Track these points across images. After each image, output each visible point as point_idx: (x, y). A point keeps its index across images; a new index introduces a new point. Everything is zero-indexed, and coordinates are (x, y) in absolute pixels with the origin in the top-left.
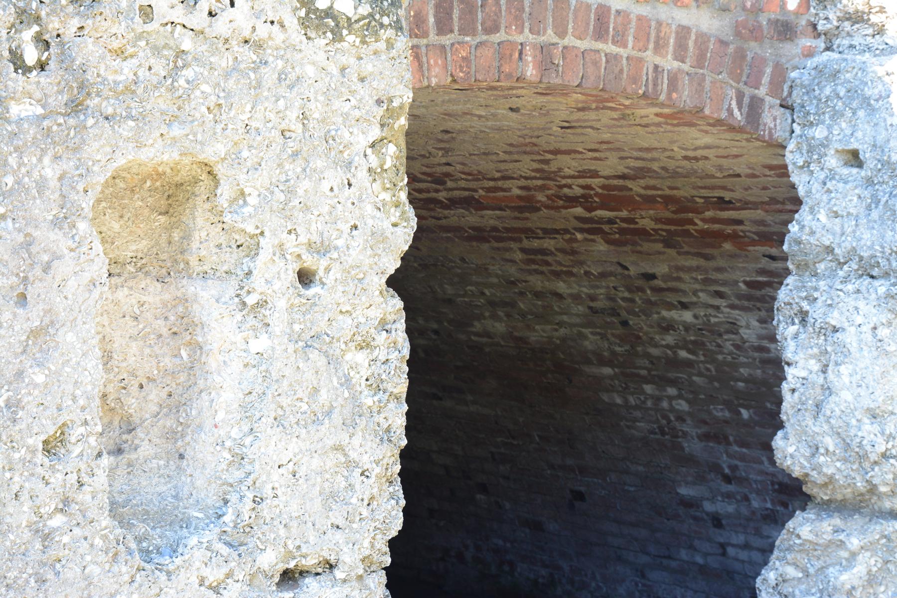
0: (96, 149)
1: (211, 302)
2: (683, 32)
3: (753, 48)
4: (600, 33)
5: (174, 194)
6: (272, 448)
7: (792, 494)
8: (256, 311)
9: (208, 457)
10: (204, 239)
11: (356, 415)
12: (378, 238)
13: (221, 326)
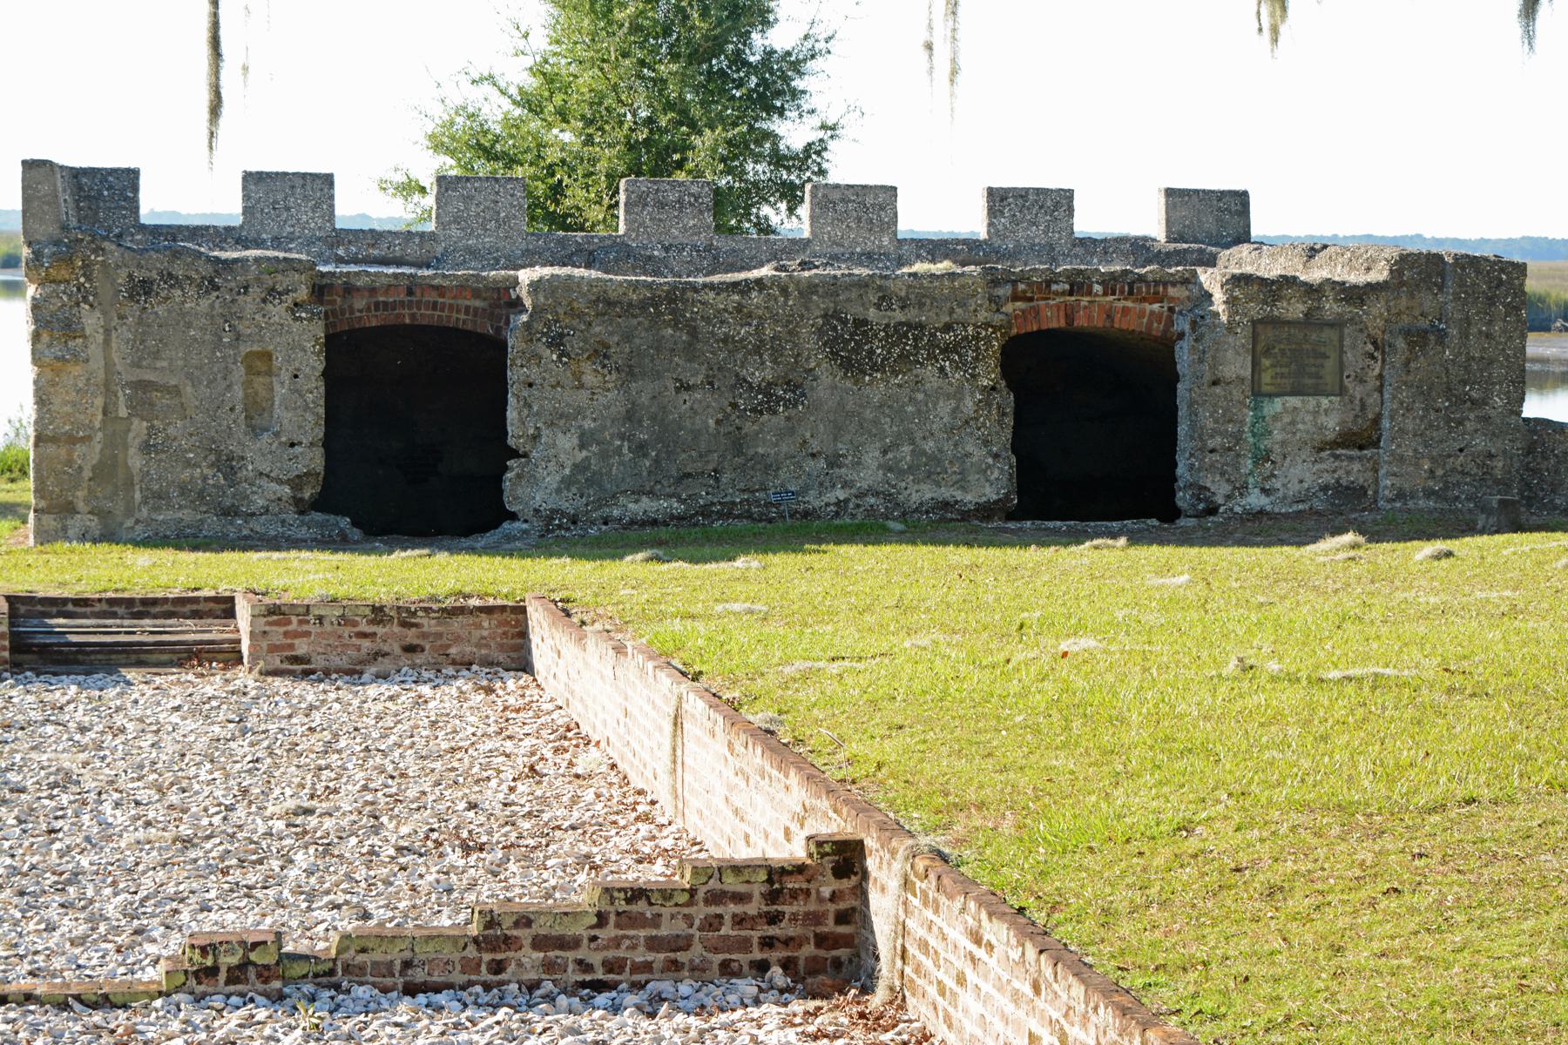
0: (242, 348)
2: (467, 308)
3: (497, 311)
11: (306, 408)
13: (277, 387)
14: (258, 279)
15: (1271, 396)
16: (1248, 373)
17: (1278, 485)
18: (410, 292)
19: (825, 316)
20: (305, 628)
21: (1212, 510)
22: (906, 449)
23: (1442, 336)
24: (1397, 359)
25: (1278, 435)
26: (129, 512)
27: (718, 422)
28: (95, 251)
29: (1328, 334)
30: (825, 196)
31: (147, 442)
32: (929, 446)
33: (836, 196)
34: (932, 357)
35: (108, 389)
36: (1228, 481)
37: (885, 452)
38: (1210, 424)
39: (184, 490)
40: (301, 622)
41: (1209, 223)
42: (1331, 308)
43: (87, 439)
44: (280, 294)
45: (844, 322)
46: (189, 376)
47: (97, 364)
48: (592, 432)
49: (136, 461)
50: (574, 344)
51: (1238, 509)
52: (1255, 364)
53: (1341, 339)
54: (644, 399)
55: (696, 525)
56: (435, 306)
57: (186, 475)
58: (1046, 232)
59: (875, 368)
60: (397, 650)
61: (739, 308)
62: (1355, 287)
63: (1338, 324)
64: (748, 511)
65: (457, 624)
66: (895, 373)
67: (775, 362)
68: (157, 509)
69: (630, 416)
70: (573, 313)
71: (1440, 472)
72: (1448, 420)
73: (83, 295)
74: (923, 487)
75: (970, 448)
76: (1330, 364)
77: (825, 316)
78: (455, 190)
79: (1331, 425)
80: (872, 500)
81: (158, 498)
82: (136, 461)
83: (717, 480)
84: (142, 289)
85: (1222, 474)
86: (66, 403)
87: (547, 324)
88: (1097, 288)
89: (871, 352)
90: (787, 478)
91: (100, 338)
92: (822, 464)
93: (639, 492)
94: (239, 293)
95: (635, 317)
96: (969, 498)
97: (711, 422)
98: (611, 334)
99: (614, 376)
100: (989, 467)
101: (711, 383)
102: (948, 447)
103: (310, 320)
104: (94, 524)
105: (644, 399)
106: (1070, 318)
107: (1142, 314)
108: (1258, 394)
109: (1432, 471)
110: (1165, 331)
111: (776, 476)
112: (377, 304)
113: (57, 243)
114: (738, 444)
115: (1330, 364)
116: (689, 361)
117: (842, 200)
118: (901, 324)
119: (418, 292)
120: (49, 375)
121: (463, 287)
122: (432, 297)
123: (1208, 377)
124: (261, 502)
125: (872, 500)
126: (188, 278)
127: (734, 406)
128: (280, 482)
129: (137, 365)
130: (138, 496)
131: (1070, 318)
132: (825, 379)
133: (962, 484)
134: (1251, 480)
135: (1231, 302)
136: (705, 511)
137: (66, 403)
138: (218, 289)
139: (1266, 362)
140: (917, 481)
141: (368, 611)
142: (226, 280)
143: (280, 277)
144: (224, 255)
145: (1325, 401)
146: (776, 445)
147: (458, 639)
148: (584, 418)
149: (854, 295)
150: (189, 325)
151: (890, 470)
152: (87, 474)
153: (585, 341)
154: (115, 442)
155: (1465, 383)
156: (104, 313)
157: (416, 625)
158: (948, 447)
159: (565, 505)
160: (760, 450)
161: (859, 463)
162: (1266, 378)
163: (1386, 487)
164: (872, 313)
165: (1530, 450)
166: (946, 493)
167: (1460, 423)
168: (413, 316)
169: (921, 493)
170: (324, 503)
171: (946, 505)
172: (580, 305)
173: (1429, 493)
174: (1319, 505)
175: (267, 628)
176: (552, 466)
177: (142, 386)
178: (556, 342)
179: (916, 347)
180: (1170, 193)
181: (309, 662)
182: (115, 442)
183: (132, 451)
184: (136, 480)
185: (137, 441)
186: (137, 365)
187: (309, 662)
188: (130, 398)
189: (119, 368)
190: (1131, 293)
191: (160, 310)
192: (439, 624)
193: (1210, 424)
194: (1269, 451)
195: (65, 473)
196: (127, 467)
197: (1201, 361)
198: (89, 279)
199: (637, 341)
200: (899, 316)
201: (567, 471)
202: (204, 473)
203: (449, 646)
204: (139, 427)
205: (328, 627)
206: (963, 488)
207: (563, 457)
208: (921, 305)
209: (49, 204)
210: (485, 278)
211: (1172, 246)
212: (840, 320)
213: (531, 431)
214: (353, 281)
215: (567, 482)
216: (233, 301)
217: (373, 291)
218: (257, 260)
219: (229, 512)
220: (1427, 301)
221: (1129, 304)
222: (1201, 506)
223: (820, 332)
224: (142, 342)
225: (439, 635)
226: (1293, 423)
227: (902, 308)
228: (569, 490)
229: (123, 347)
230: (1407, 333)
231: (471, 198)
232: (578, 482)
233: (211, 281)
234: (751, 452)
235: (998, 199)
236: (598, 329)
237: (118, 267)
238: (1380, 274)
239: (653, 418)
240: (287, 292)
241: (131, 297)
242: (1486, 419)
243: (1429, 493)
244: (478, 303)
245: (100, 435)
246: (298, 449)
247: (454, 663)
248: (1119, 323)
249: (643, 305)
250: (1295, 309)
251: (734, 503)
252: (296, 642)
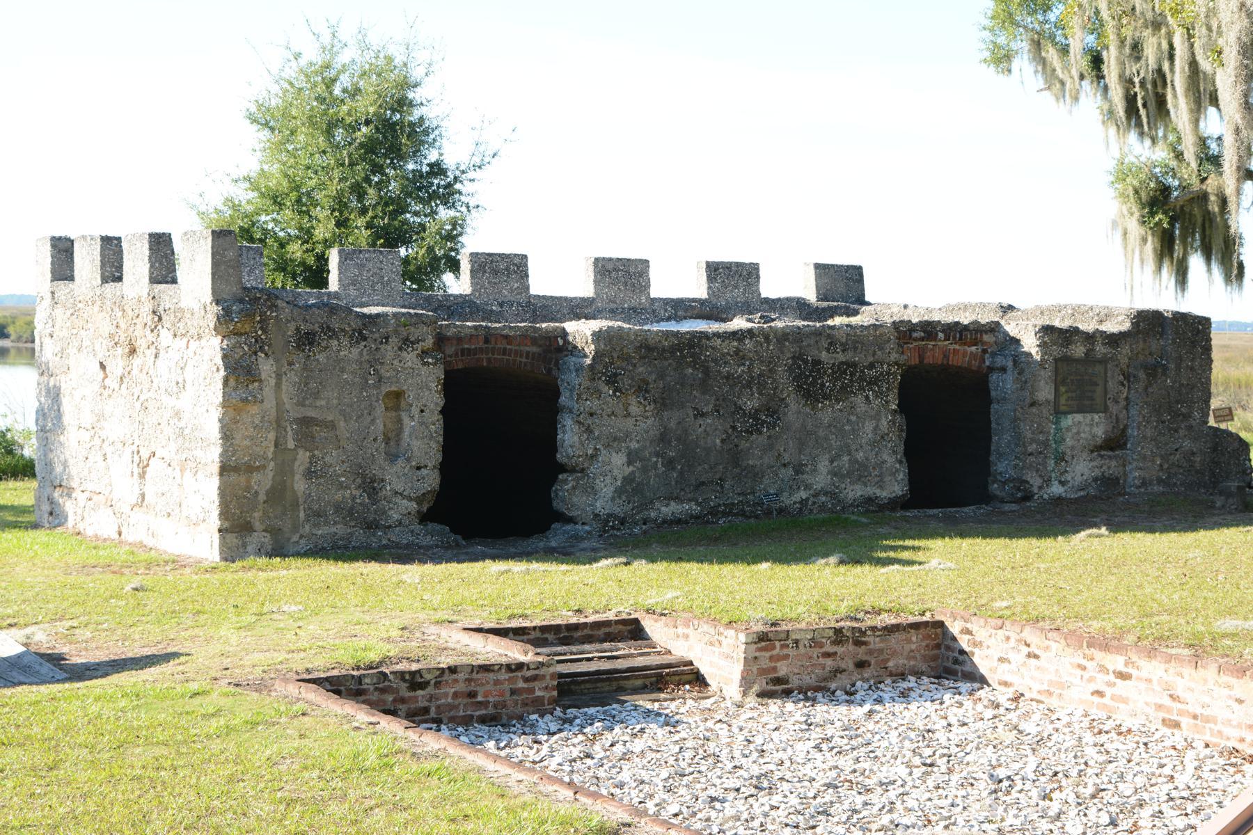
1: (404, 416)
2: (528, 353)
4: (504, 354)
5: (398, 395)
6: (417, 445)
7: (563, 469)
8: (412, 418)
9: (404, 444)
10: (403, 404)
11: (431, 437)
12: (437, 404)
13: (406, 420)
14: (396, 331)
16: (1051, 397)
17: (1069, 478)
18: (487, 341)
19: (793, 358)
20: (785, 651)
21: (1028, 497)
22: (846, 458)
23: (1165, 368)
24: (1140, 386)
25: (1069, 442)
26: (295, 529)
27: (723, 441)
28: (270, 308)
29: (1099, 368)
30: (603, 266)
31: (309, 469)
32: (860, 455)
33: (610, 266)
34: (862, 388)
35: (279, 424)
37: (832, 462)
38: (1029, 435)
39: (338, 508)
40: (782, 646)
41: (841, 287)
42: (1100, 349)
44: (413, 343)
45: (806, 362)
46: (342, 413)
47: (270, 404)
48: (637, 451)
49: (300, 485)
50: (625, 382)
51: (1046, 496)
52: (1056, 390)
53: (1106, 373)
54: (672, 425)
55: (708, 522)
56: (504, 352)
57: (339, 496)
58: (744, 294)
59: (826, 397)
60: (851, 666)
61: (737, 352)
62: (1113, 334)
63: (1104, 361)
64: (743, 510)
65: (894, 640)
66: (838, 401)
67: (760, 394)
68: (316, 525)
69: (663, 438)
70: (626, 358)
71: (1166, 466)
72: (1170, 429)
73: (260, 346)
74: (857, 487)
75: (885, 457)
76: (1099, 389)
77: (793, 358)
78: (352, 259)
79: (1100, 433)
80: (824, 499)
81: (317, 515)
82: (300, 485)
83: (722, 486)
84: (306, 340)
85: (1037, 471)
86: (245, 438)
87: (606, 367)
88: (941, 335)
89: (823, 385)
90: (768, 485)
91: (273, 382)
92: (791, 472)
93: (669, 498)
94: (381, 343)
95: (666, 359)
96: (884, 494)
97: (718, 441)
98: (650, 373)
99: (653, 406)
100: (897, 470)
101: (718, 411)
102: (872, 456)
103: (435, 364)
104: (267, 539)
105: (672, 425)
106: (921, 358)
107: (965, 353)
109: (1161, 465)
110: (980, 367)
111: (761, 483)
112: (463, 350)
113: (241, 301)
114: (735, 457)
115: (1099, 389)
116: (703, 393)
117: (615, 269)
118: (842, 363)
119: (493, 340)
120: (232, 413)
121: (525, 336)
122: (502, 345)
123: (1028, 401)
124: (396, 516)
125: (824, 499)
126: (343, 330)
127: (734, 428)
128: (410, 499)
129: (301, 404)
130: (302, 515)
131: (921, 358)
132: (793, 406)
133: (880, 484)
135: (1043, 345)
136: (714, 512)
137: (245, 438)
138: (365, 339)
139: (1063, 389)
140: (852, 483)
141: (831, 633)
142: (371, 332)
143: (412, 329)
144: (366, 310)
145: (1096, 417)
146: (761, 458)
147: (894, 653)
148: (631, 440)
149: (812, 342)
150: (343, 370)
151: (835, 475)
152: (262, 497)
153: (632, 379)
154: (284, 470)
155: (1178, 402)
156: (277, 361)
157: (865, 643)
158: (872, 456)
159: (617, 510)
160: (751, 462)
161: (815, 470)
162: (1063, 401)
163: (1135, 478)
164: (824, 355)
165: (1214, 449)
166: (871, 491)
167: (1176, 431)
168: (489, 360)
171: (870, 500)
172: (630, 350)
173: (1160, 481)
174: (1092, 492)
175: (757, 654)
176: (608, 480)
177: (305, 422)
178: (612, 380)
179: (851, 381)
180: (818, 266)
181: (787, 682)
182: (284, 470)
183: (297, 477)
184: (301, 501)
185: (302, 468)
186: (301, 404)
187: (787, 682)
188: (296, 433)
189: (287, 407)
190: (961, 339)
191: (321, 357)
192: (882, 641)
193: (1029, 435)
194: (1064, 453)
195: (245, 497)
196: (294, 492)
197: (1022, 389)
198: (265, 331)
199: (668, 379)
200: (841, 357)
201: (619, 483)
202: (352, 494)
203: (888, 660)
204: (303, 456)
205: (802, 650)
206: (881, 487)
207: (616, 472)
208: (855, 348)
209: (233, 267)
210: (540, 329)
211: (825, 304)
212: (803, 360)
213: (590, 452)
214: (444, 332)
215: (619, 492)
216: (377, 349)
217: (459, 340)
218: (395, 315)
219: (372, 526)
220: (1155, 345)
221: (957, 347)
222: (1019, 495)
223: (790, 370)
224: (306, 384)
225: (881, 651)
226: (1078, 433)
227: (843, 351)
228: (620, 498)
229: (291, 389)
230: (1145, 367)
231: (363, 266)
232: (627, 491)
233: (360, 333)
234: (744, 464)
235: (715, 271)
236: (641, 369)
237: (288, 321)
238: (1126, 326)
239: (678, 439)
240: (418, 341)
241: (298, 347)
242: (1190, 428)
243: (1160, 481)
244: (535, 349)
245: (272, 464)
246: (424, 472)
247: (891, 675)
248: (955, 361)
249: (673, 349)
250: (1079, 350)
251: (733, 504)
252: (778, 664)
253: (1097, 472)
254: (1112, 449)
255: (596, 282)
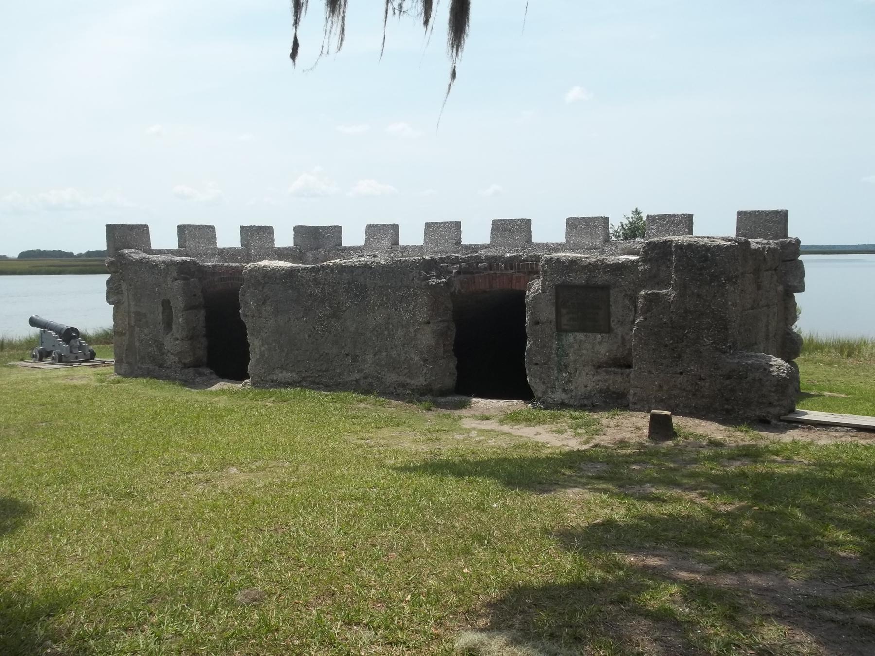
15: (567, 331)
16: (553, 317)
17: (572, 388)
22: (384, 354)
27: (309, 336)
32: (394, 353)
36: (544, 383)
37: (375, 355)
42: (601, 278)
43: (125, 334)
61: (315, 280)
63: (605, 288)
68: (142, 363)
71: (665, 388)
75: (412, 355)
77: (349, 283)
79: (603, 351)
82: (137, 344)
85: (540, 379)
93: (282, 368)
96: (413, 382)
97: (306, 336)
108: (560, 330)
134: (557, 383)
139: (564, 311)
162: (564, 320)
169: (391, 378)
170: (196, 365)
219: (161, 366)
250: (579, 279)
253: (601, 385)
254: (621, 367)
255: (567, 234)
